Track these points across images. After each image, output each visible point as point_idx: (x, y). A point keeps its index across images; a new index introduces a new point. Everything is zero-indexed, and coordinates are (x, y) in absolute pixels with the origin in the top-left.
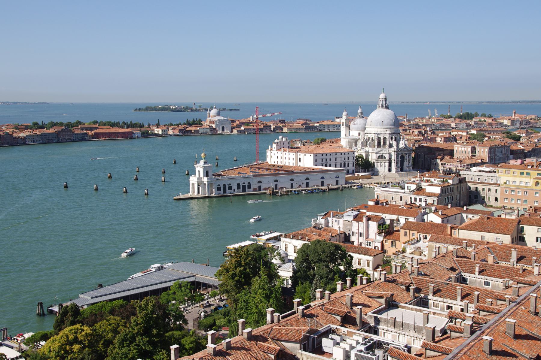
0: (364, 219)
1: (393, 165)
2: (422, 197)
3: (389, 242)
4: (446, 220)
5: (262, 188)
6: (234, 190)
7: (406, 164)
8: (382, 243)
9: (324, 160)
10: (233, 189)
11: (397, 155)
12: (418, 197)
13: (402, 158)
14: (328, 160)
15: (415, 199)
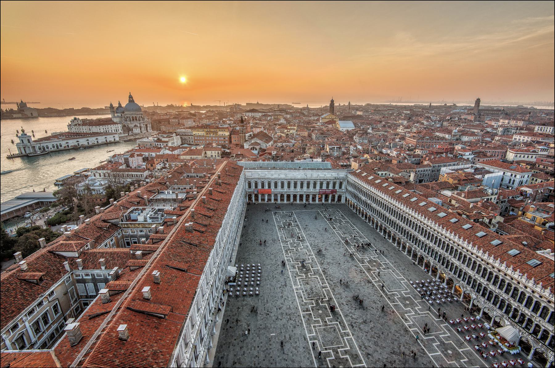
0: (136, 156)
1: (143, 129)
2: (161, 144)
3: (150, 165)
4: (173, 152)
5: (70, 146)
6: (51, 148)
7: (148, 128)
8: (146, 165)
9: (105, 129)
10: (50, 148)
11: (144, 125)
12: (159, 144)
13: (146, 125)
14: (107, 129)
15: (158, 145)
